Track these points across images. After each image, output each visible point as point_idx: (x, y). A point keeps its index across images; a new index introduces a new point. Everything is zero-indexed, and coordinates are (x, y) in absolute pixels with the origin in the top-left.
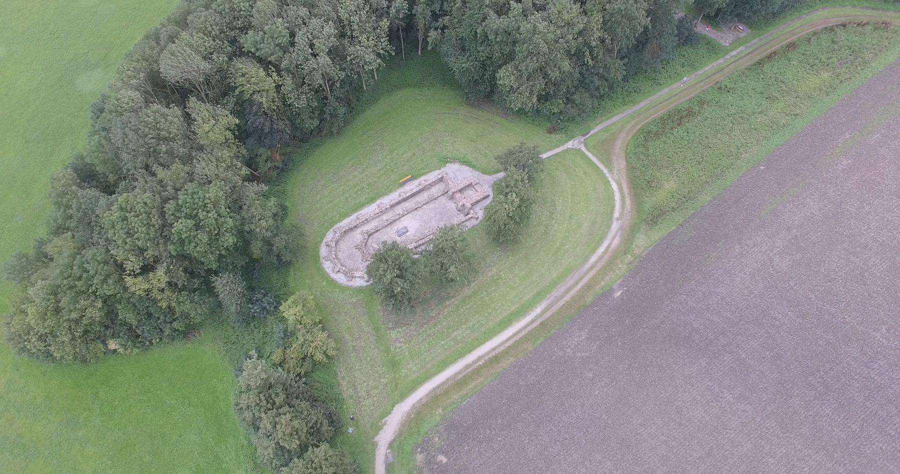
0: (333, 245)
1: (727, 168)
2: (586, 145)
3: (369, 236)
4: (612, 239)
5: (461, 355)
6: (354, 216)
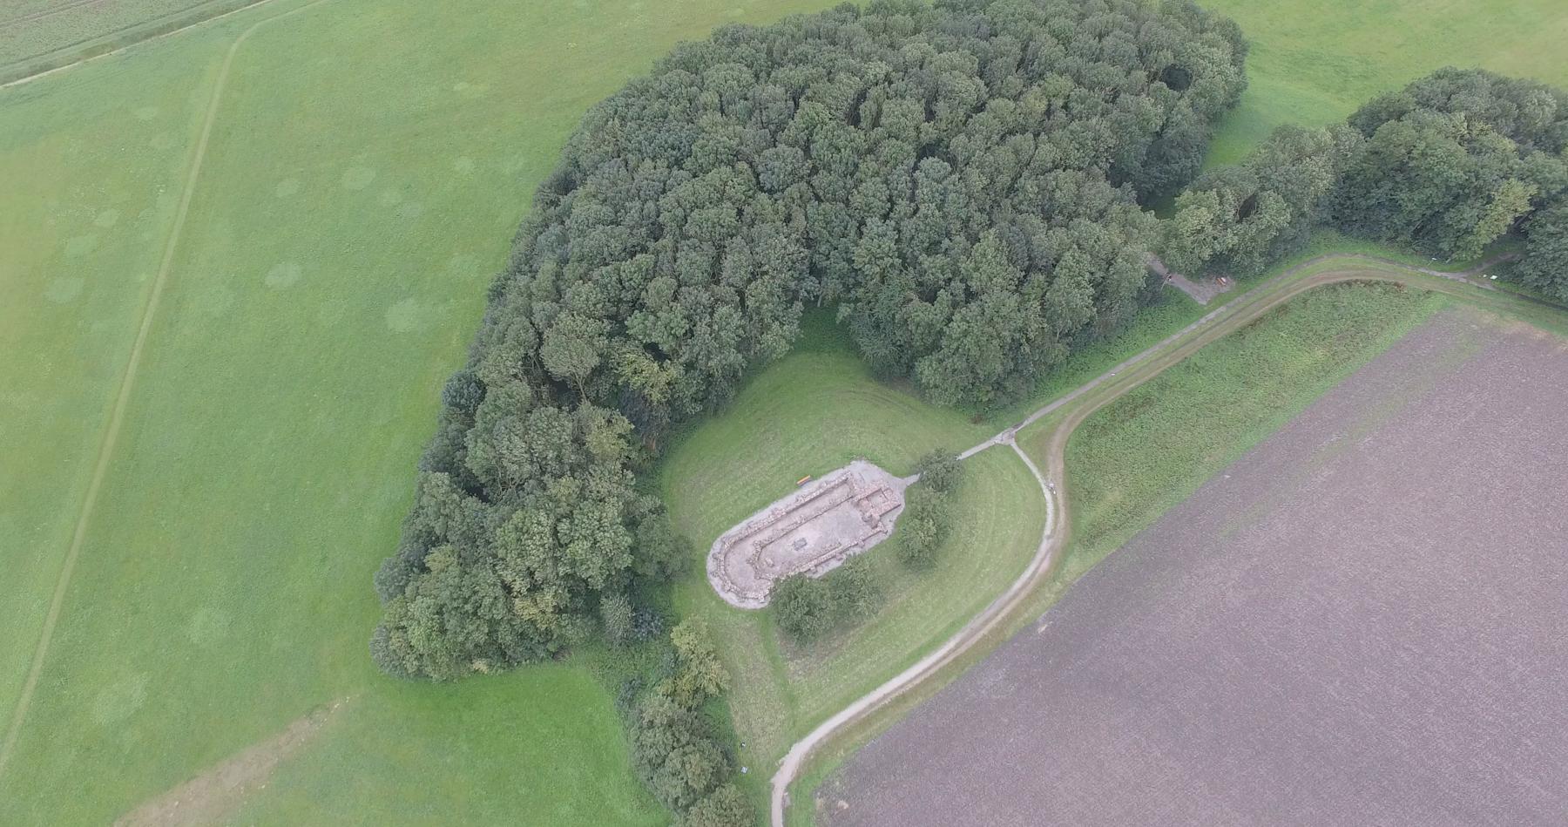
0: (722, 559)
1: (1185, 476)
2: (1017, 441)
3: (762, 548)
4: (1040, 563)
5: (866, 691)
6: (744, 524)
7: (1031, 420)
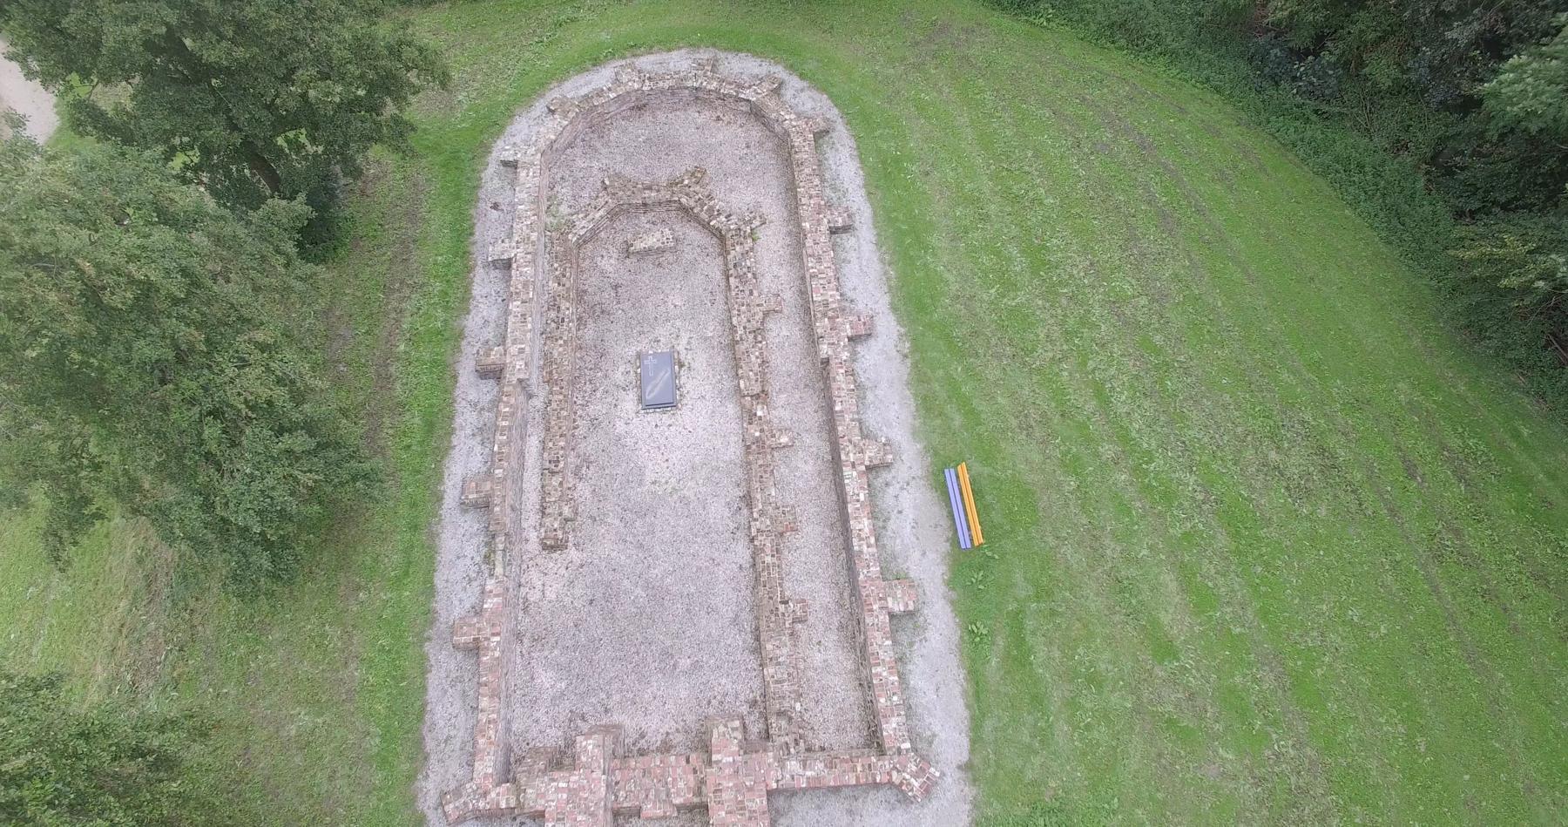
6: (858, 202)
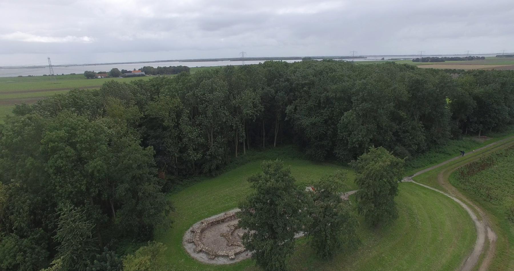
6: (222, 214)
7: (418, 174)
